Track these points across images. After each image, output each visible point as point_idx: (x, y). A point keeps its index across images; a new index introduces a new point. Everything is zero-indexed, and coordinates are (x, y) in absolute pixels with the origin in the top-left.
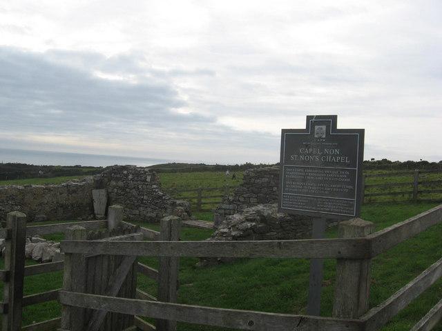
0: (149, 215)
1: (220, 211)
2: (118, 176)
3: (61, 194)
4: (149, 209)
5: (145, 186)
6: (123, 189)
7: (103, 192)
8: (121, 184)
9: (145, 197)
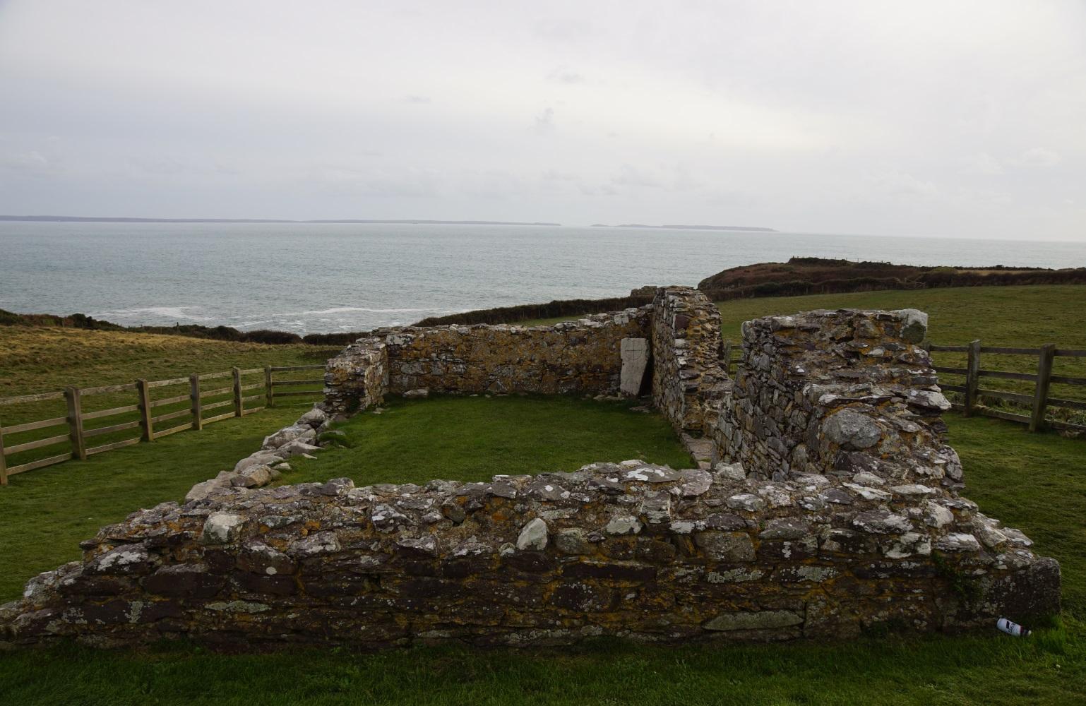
7: (641, 343)
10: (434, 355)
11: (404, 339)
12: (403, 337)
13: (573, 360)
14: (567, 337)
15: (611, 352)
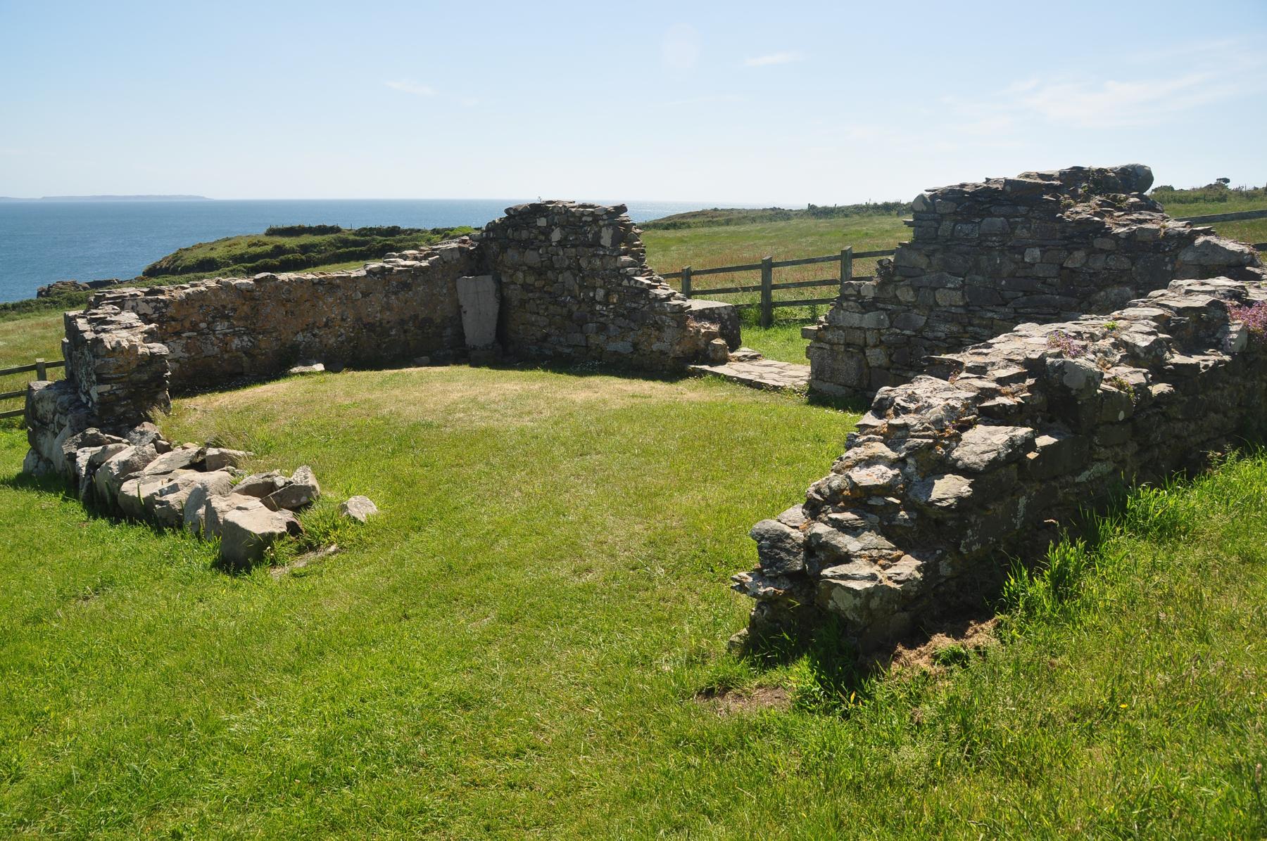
0: (612, 347)
3: (365, 295)
6: (539, 272)
7: (487, 282)
8: (532, 257)
10: (203, 325)
11: (154, 304)
12: (152, 300)
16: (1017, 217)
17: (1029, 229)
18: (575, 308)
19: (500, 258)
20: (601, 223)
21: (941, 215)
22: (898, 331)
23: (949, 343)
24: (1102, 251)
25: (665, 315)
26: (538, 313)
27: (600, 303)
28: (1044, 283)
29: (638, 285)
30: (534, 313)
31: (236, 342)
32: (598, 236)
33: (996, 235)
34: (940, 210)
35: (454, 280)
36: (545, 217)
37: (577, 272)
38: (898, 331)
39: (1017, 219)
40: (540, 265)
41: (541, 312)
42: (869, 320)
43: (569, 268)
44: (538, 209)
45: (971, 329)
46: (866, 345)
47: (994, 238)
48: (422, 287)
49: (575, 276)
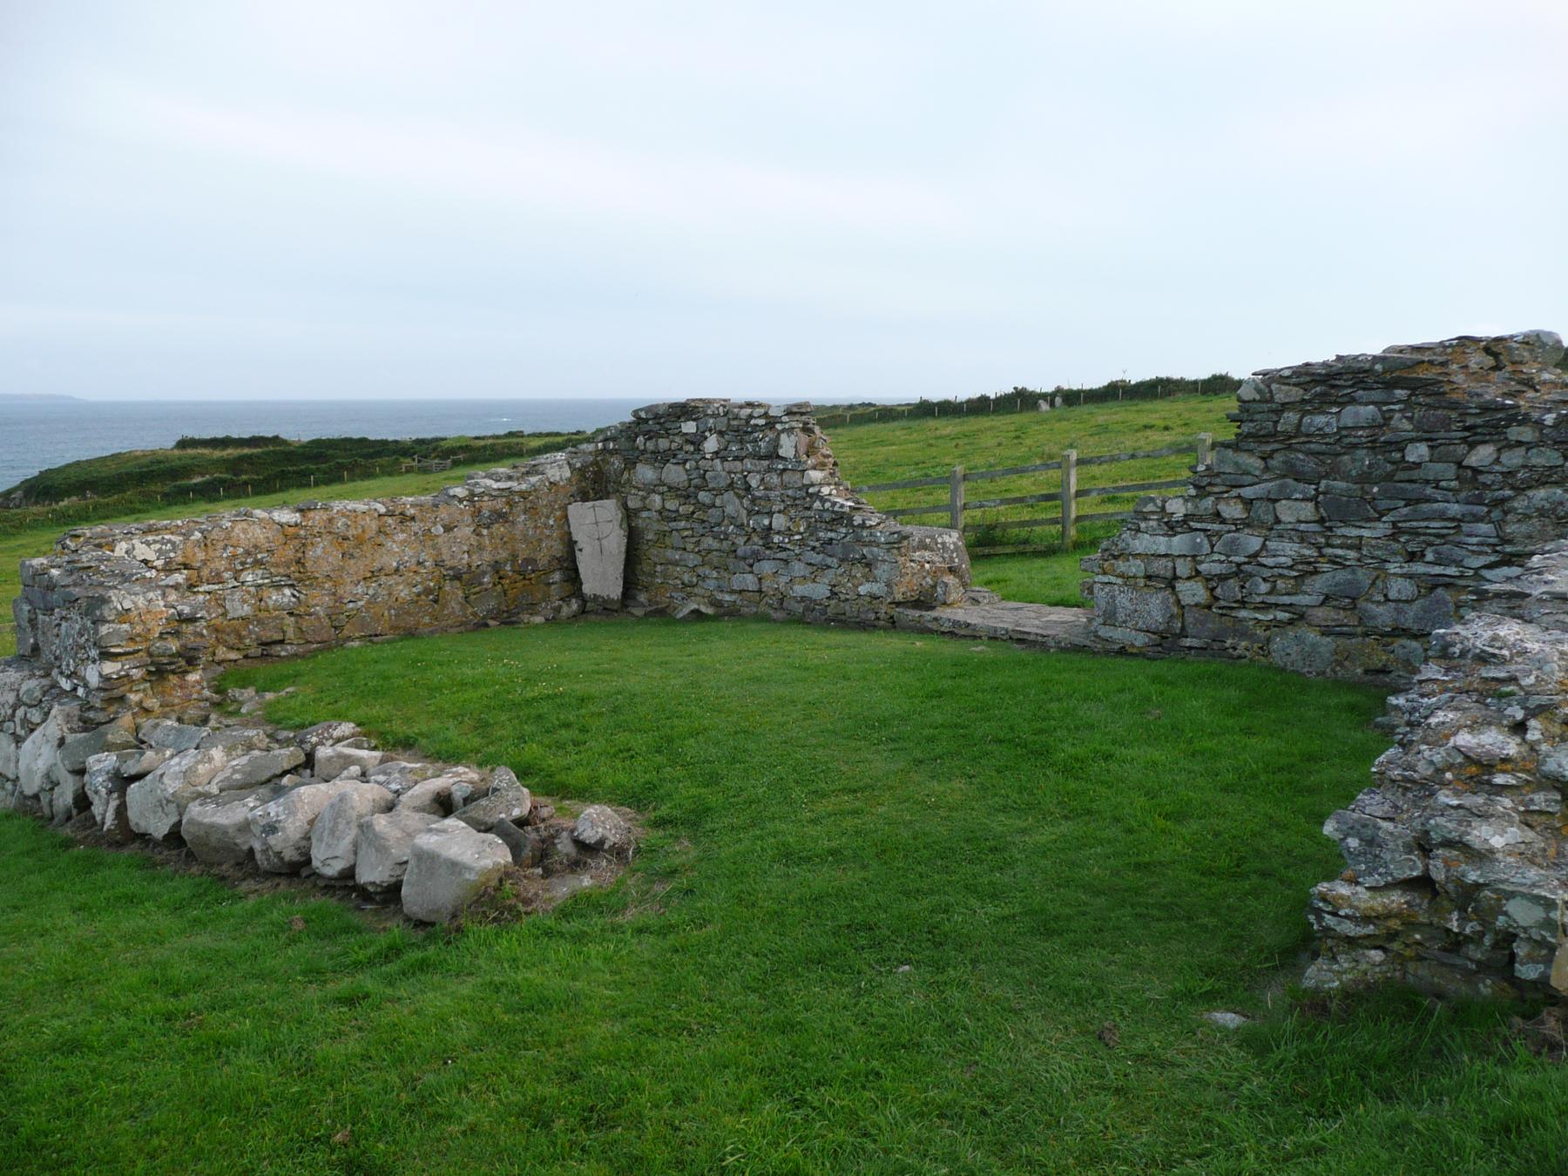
0: (799, 590)
1: (1121, 566)
2: (663, 444)
3: (448, 529)
4: (798, 568)
5: (774, 479)
6: (686, 495)
7: (608, 509)
8: (675, 474)
9: (779, 521)
11: (158, 546)
13: (487, 557)
14: (478, 513)
15: (547, 532)
16: (1393, 404)
17: (1410, 419)
18: (741, 541)
19: (626, 475)
20: (779, 427)
21: (1283, 405)
22: (1223, 558)
23: (1299, 571)
24: (1520, 443)
25: (878, 546)
26: (685, 549)
27: (778, 533)
28: (1437, 487)
29: (836, 509)
30: (678, 549)
31: (274, 597)
32: (776, 444)
33: (1362, 428)
34: (1280, 397)
35: (564, 508)
36: (694, 420)
37: (742, 493)
38: (1223, 558)
39: (1392, 407)
40: (686, 484)
41: (690, 547)
42: (1179, 543)
43: (731, 486)
44: (684, 410)
45: (1329, 551)
46: (1175, 578)
47: (1360, 433)
48: (523, 517)
49: (740, 497)
